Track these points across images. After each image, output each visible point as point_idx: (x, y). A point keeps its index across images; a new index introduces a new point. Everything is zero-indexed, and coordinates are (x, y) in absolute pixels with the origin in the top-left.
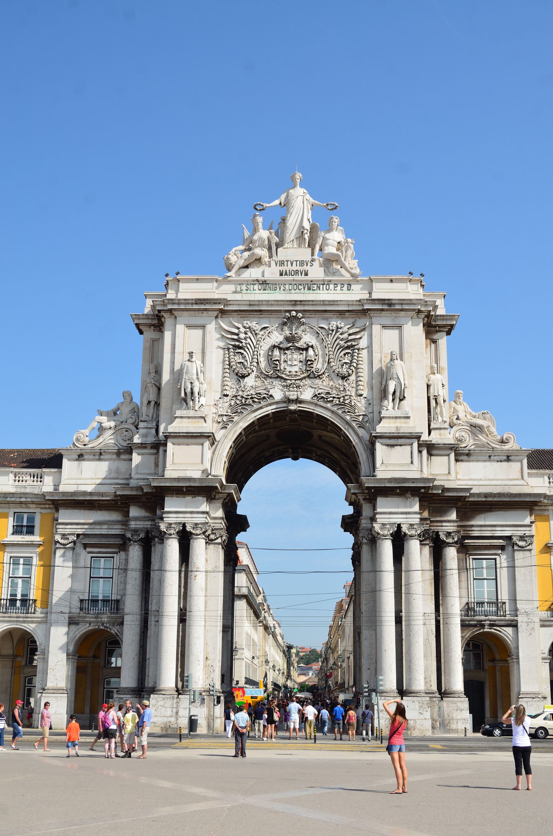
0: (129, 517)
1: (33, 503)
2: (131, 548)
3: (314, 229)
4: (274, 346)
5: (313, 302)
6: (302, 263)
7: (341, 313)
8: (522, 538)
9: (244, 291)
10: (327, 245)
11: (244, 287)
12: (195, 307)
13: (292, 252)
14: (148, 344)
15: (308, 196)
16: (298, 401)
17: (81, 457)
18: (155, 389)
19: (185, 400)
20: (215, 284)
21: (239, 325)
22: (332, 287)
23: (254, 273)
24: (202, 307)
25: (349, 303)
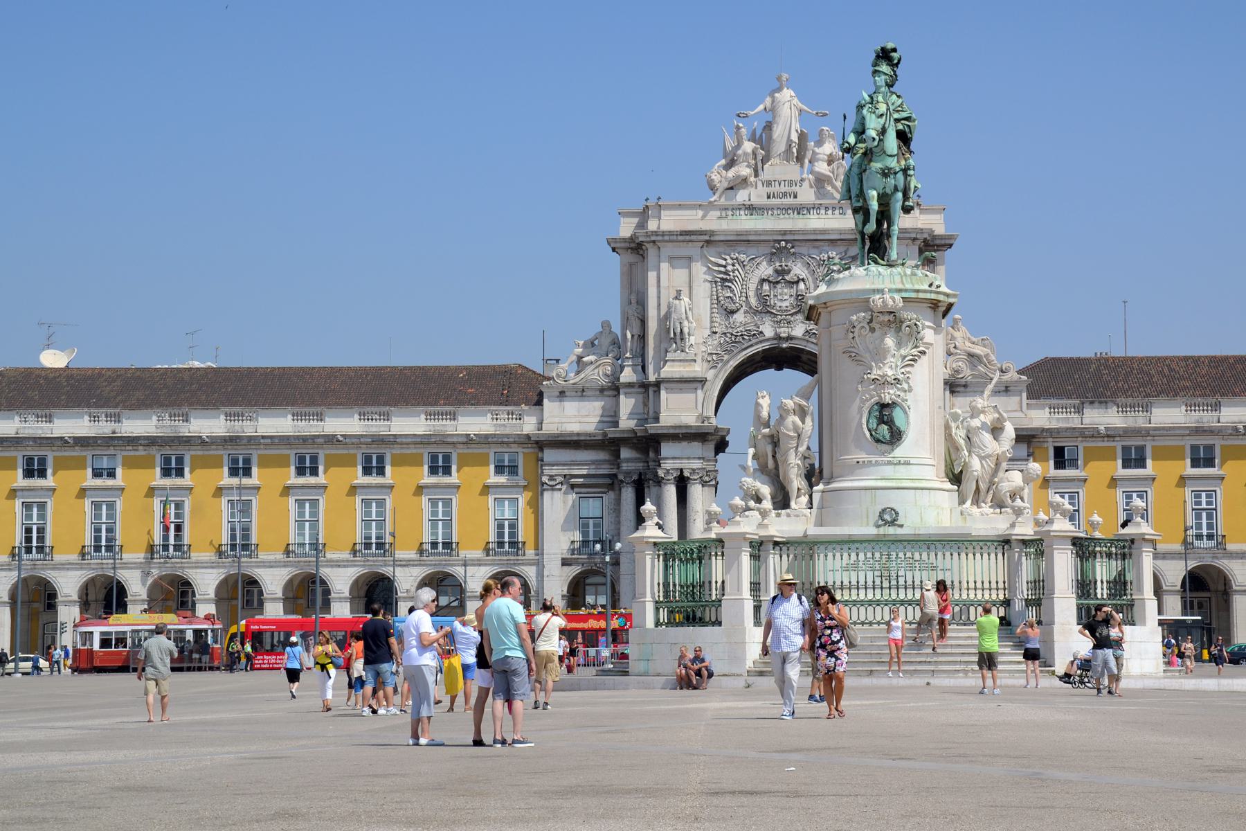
0: (618, 456)
2: (623, 490)
3: (802, 137)
4: (764, 280)
5: (804, 232)
6: (791, 183)
7: (833, 242)
10: (818, 160)
12: (680, 238)
13: (777, 169)
15: (796, 101)
16: (790, 338)
18: (639, 322)
19: (674, 339)
20: (700, 213)
22: (823, 211)
23: (742, 196)
24: (688, 238)
25: (841, 232)
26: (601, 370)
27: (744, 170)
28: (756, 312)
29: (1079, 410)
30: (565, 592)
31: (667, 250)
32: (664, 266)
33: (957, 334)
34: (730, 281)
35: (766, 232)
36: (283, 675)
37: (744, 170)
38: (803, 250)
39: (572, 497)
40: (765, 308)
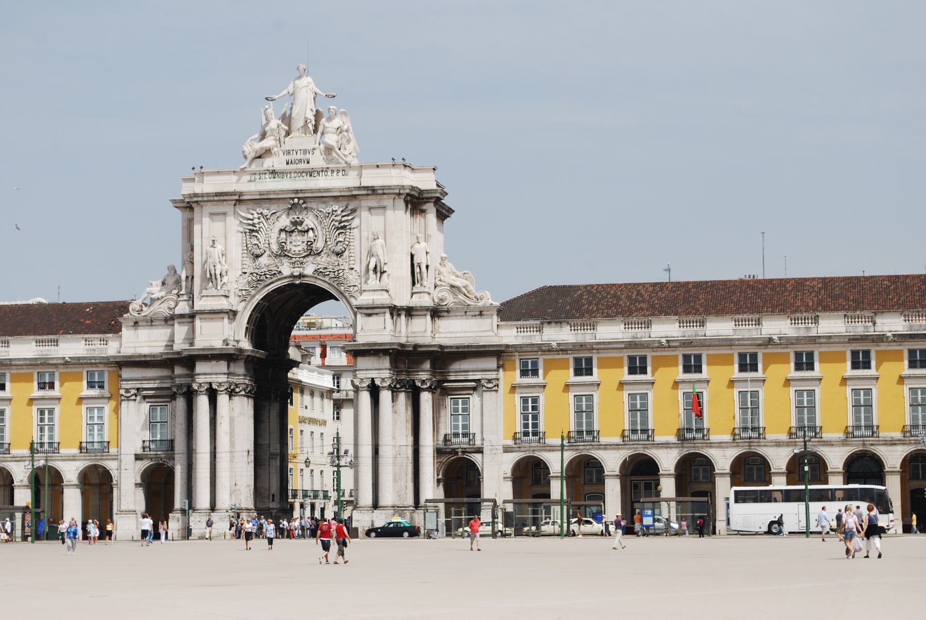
1: (101, 363)
3: (318, 115)
4: (281, 230)
5: (311, 191)
6: (305, 152)
7: (336, 198)
8: (489, 381)
9: (258, 180)
10: (327, 133)
11: (257, 177)
12: (216, 198)
13: (299, 141)
14: (185, 224)
16: (301, 276)
17: (136, 323)
21: (253, 214)
22: (329, 173)
24: (222, 198)
26: (165, 305)
27: (268, 143)
28: (276, 256)
29: (540, 330)
30: (139, 481)
31: (209, 208)
32: (206, 220)
33: (443, 269)
34: (257, 231)
35: (282, 192)
36: (266, 541)
37: (268, 143)
38: (313, 205)
39: (145, 407)
40: (283, 253)
